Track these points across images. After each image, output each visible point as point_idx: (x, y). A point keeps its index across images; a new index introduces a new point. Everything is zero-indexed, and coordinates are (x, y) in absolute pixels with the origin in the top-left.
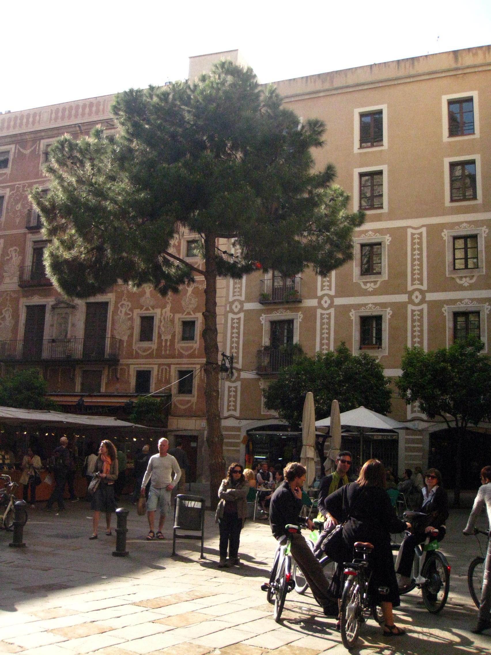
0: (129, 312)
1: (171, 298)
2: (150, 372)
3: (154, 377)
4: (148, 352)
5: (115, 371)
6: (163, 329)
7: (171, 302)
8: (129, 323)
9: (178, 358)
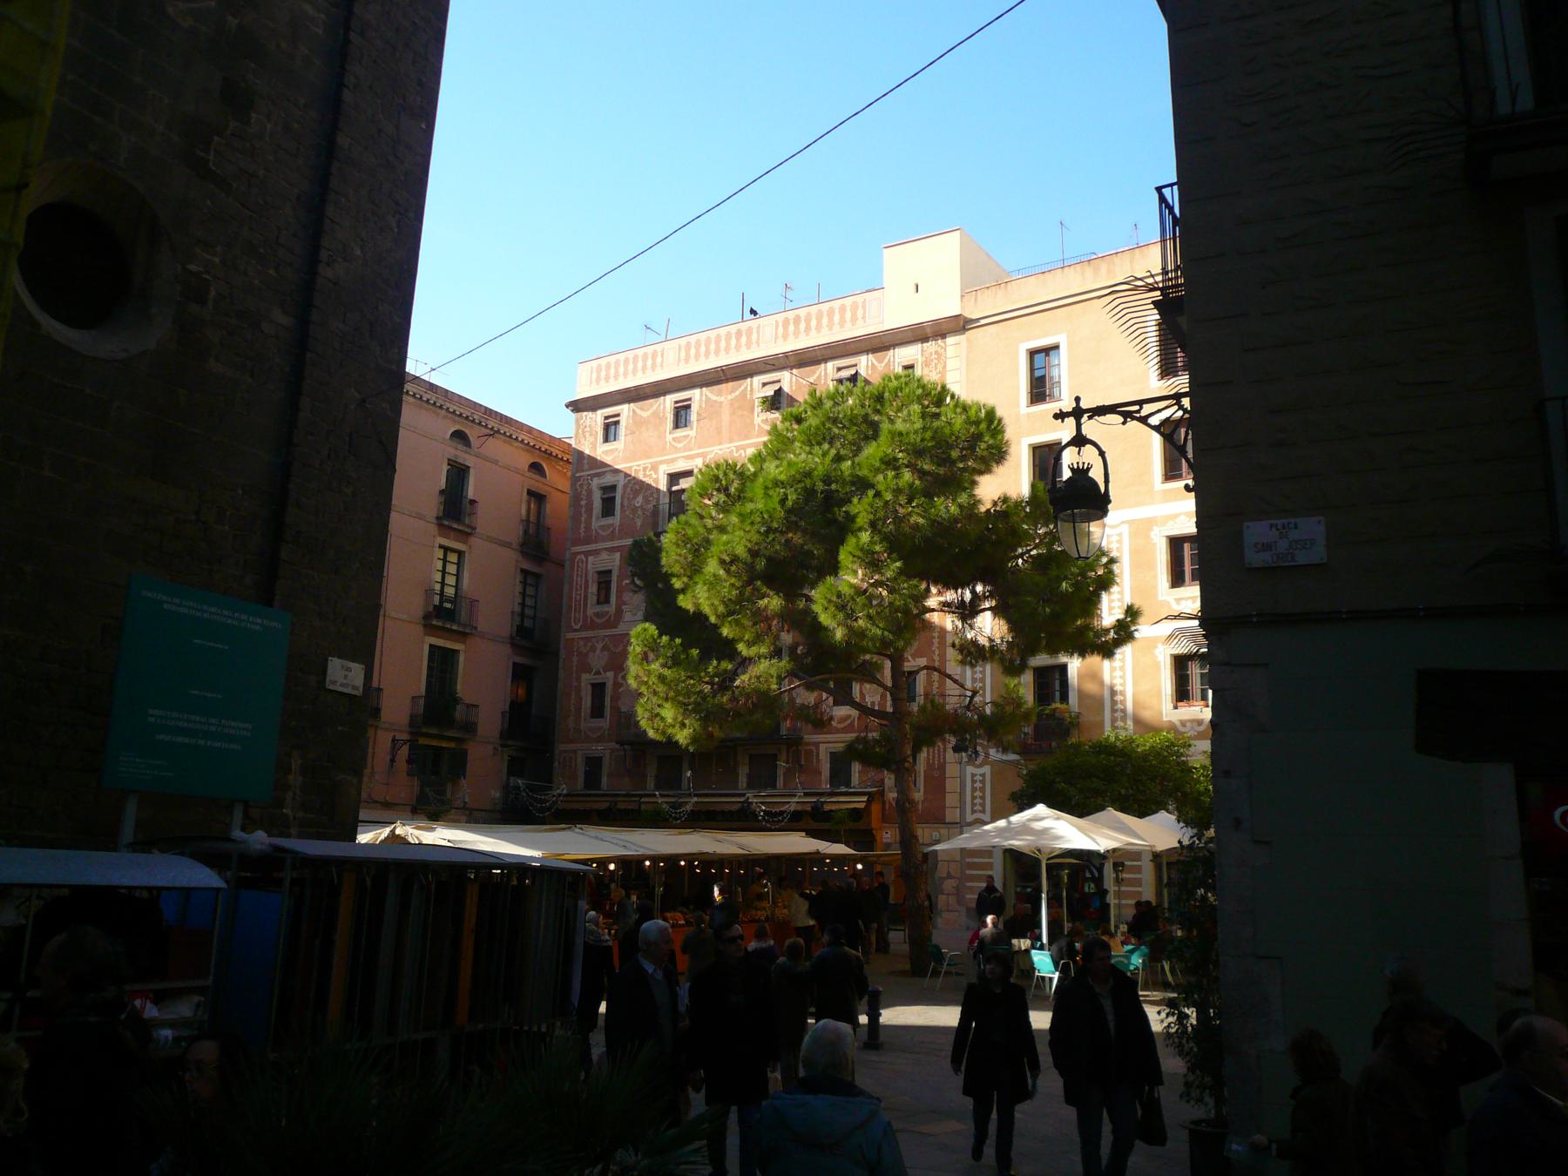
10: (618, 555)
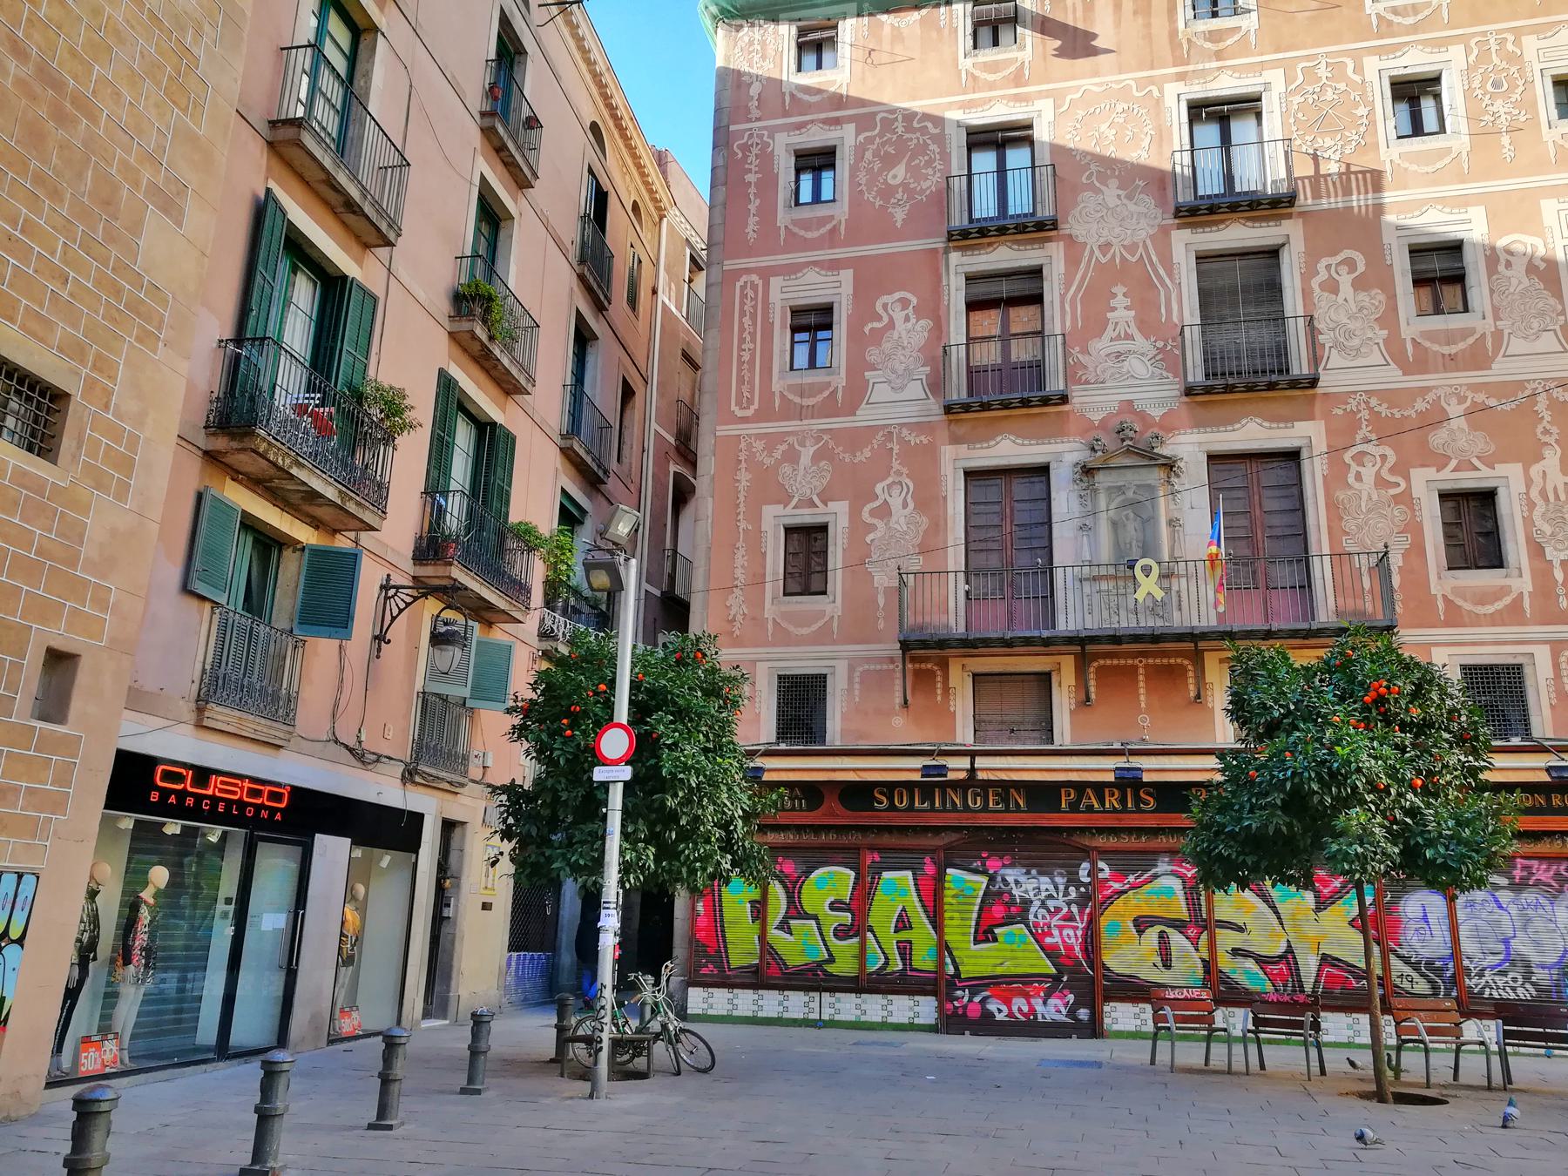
0: (1393, 479)
1: (1554, 430)
4: (1499, 605)
6: (1548, 529)
7: (1557, 441)
8: (1397, 512)
10: (847, 276)
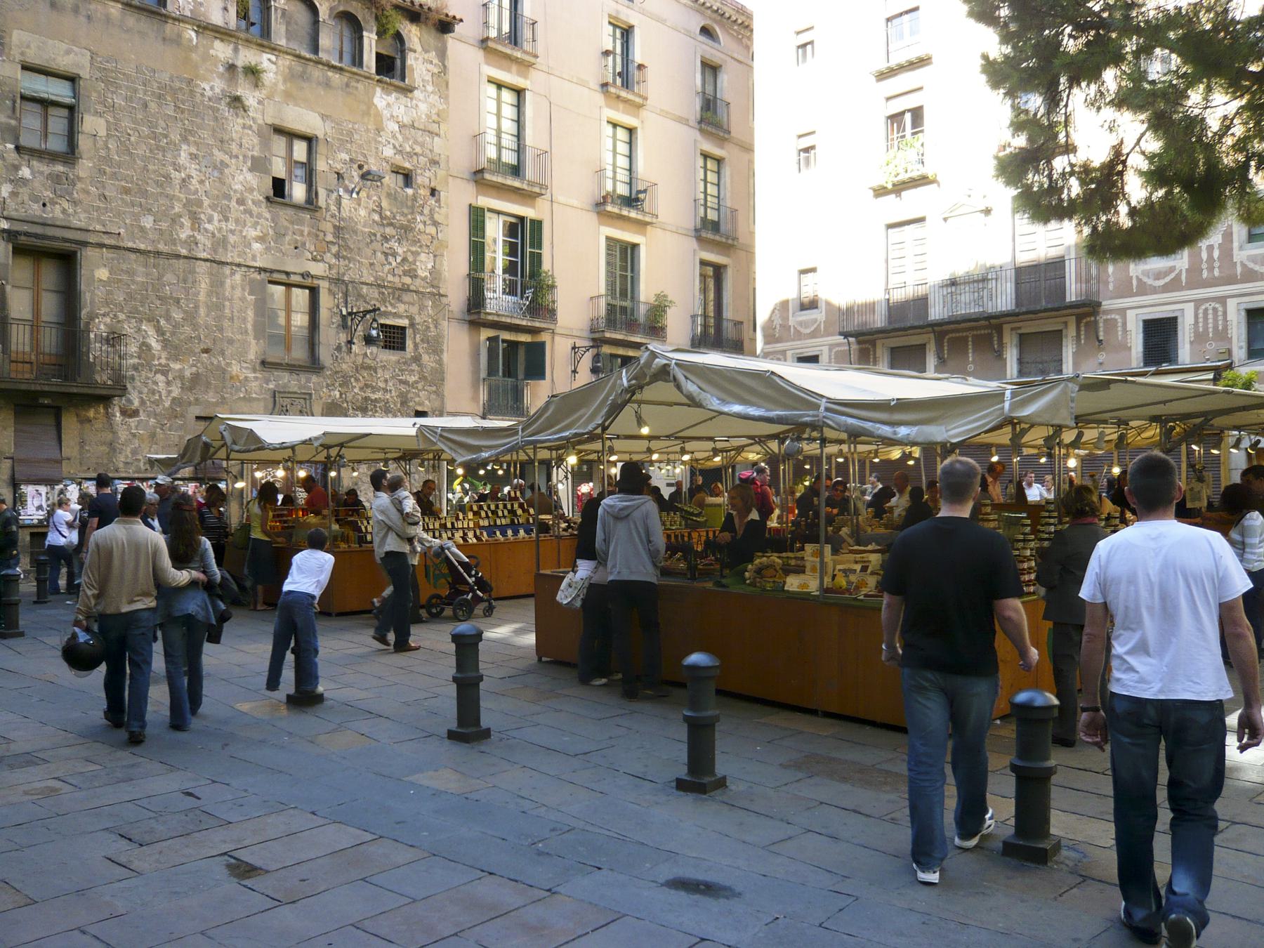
2: (1175, 319)
3: (1187, 328)
4: (1167, 279)
5: (1093, 327)
9: (1242, 282)
